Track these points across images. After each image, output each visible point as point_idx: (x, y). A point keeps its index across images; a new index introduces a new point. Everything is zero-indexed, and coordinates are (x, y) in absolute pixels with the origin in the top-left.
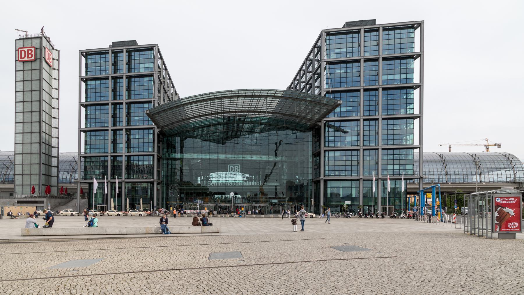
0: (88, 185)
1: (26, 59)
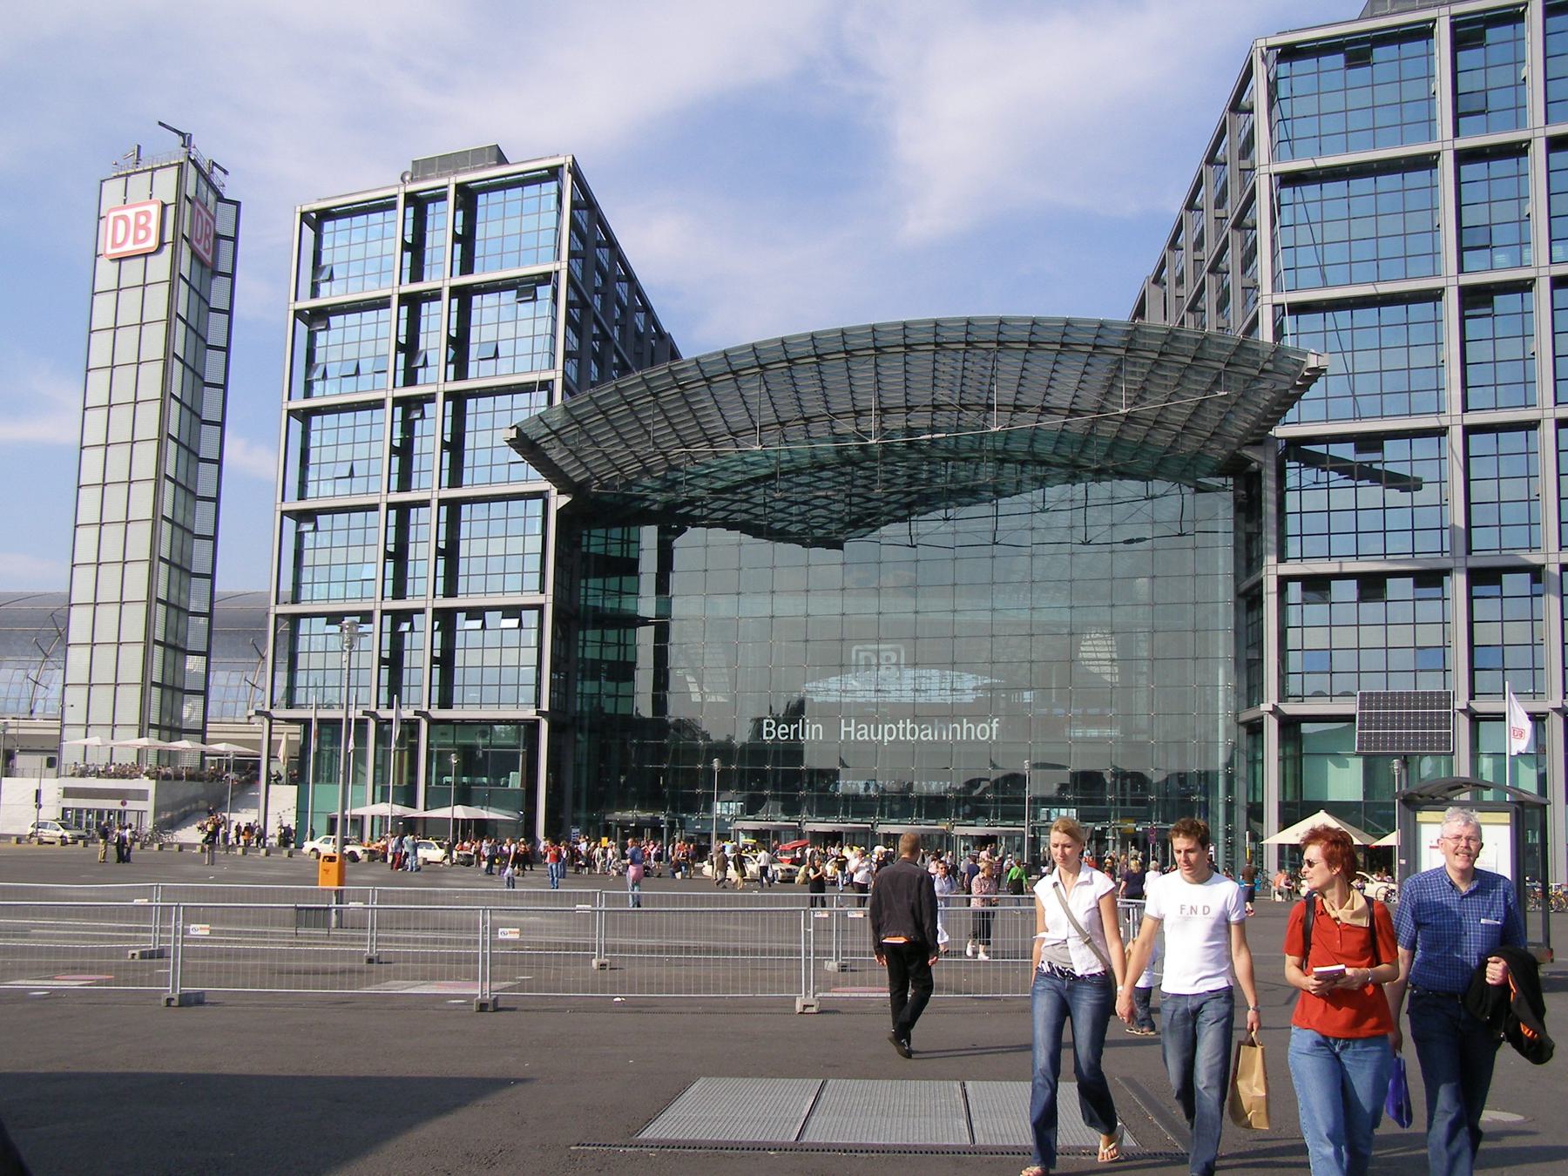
0: (298, 728)
1: (129, 247)
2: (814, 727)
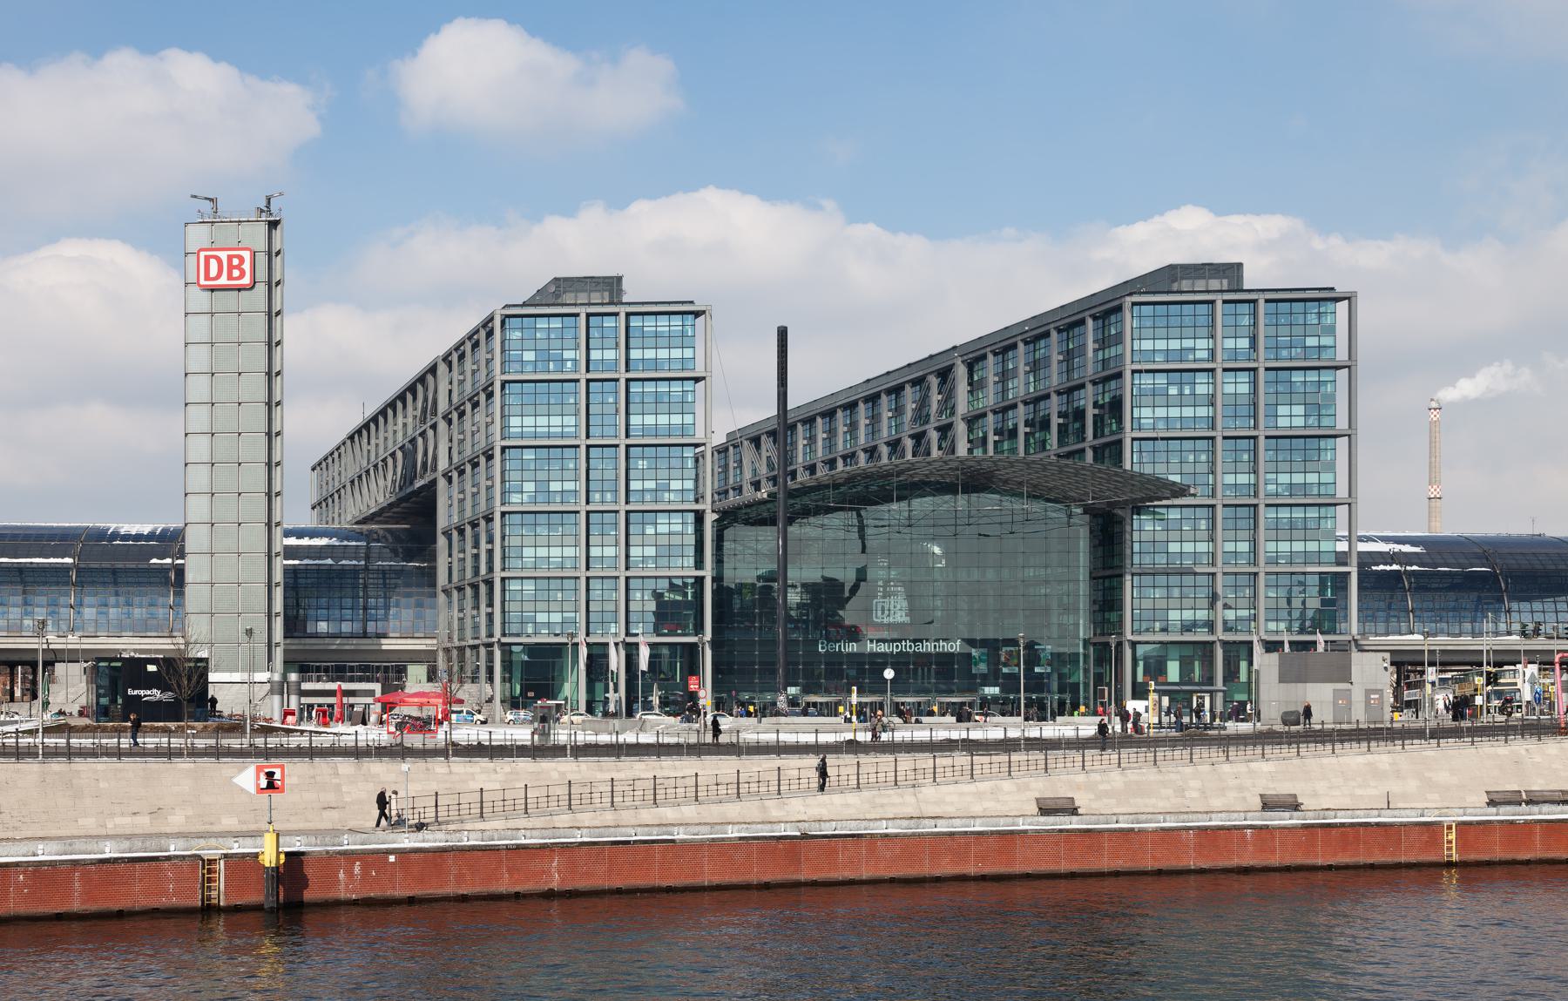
1: (223, 281)
2: (851, 644)
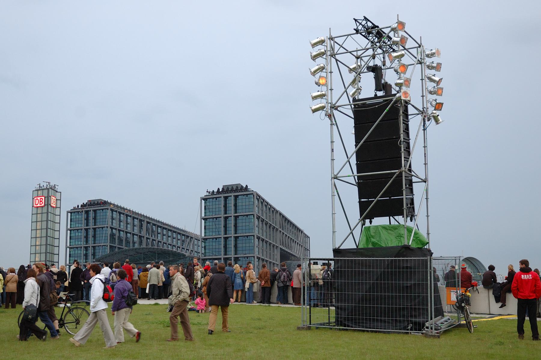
1: (39, 205)
